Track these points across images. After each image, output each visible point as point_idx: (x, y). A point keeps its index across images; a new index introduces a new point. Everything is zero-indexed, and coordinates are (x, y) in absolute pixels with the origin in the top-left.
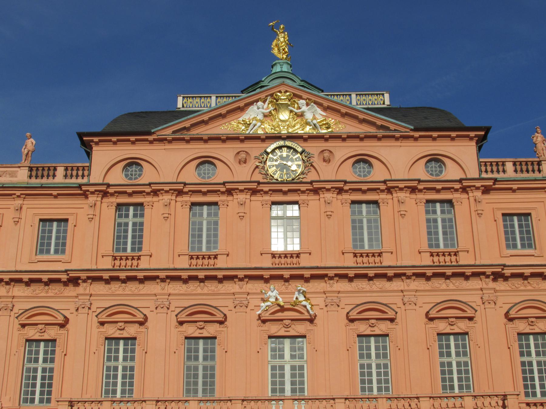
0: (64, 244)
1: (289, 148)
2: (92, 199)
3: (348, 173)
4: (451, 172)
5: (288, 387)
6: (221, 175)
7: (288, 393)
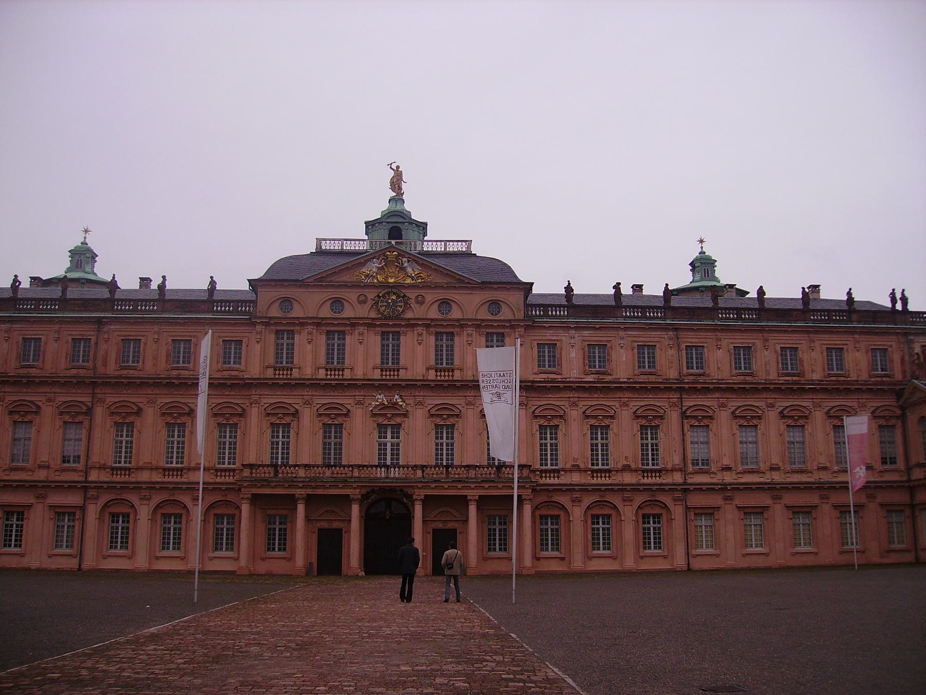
0: (240, 358)
2: (259, 328)
3: (434, 313)
4: (505, 314)
5: (389, 457)
6: (348, 313)
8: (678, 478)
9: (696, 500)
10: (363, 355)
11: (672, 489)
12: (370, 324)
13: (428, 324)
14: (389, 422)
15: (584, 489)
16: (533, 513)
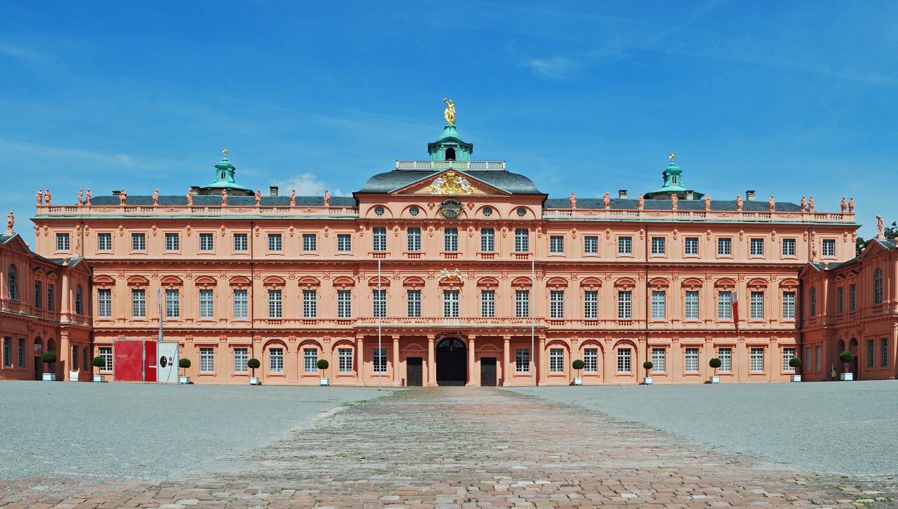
1: (453, 202)
3: (481, 216)
4: (529, 216)
6: (421, 215)
7: (451, 314)
8: (642, 326)
9: (652, 341)
10: (433, 245)
11: (637, 334)
12: (437, 224)
13: (476, 223)
14: (451, 289)
15: (580, 333)
16: (546, 348)
